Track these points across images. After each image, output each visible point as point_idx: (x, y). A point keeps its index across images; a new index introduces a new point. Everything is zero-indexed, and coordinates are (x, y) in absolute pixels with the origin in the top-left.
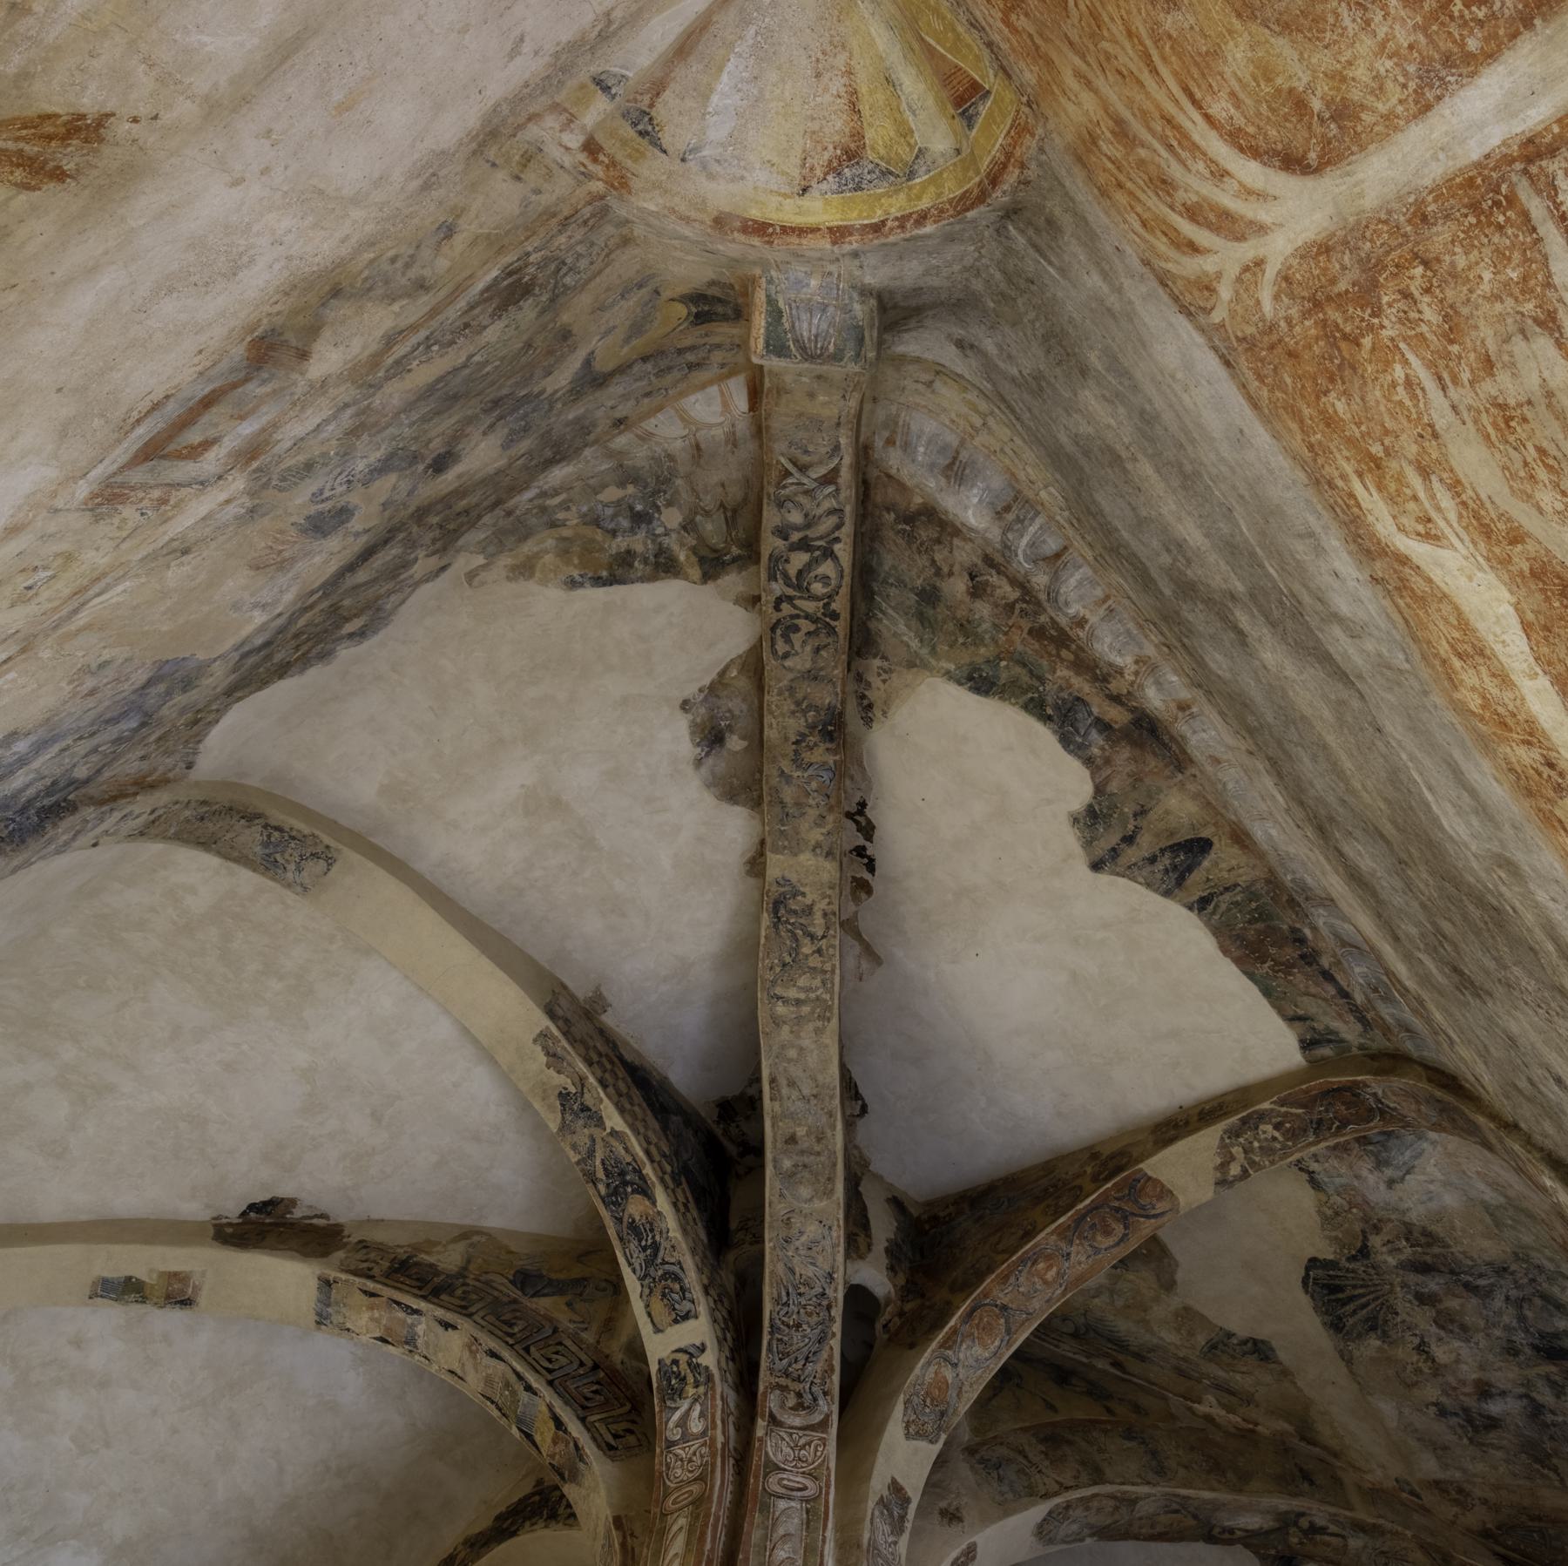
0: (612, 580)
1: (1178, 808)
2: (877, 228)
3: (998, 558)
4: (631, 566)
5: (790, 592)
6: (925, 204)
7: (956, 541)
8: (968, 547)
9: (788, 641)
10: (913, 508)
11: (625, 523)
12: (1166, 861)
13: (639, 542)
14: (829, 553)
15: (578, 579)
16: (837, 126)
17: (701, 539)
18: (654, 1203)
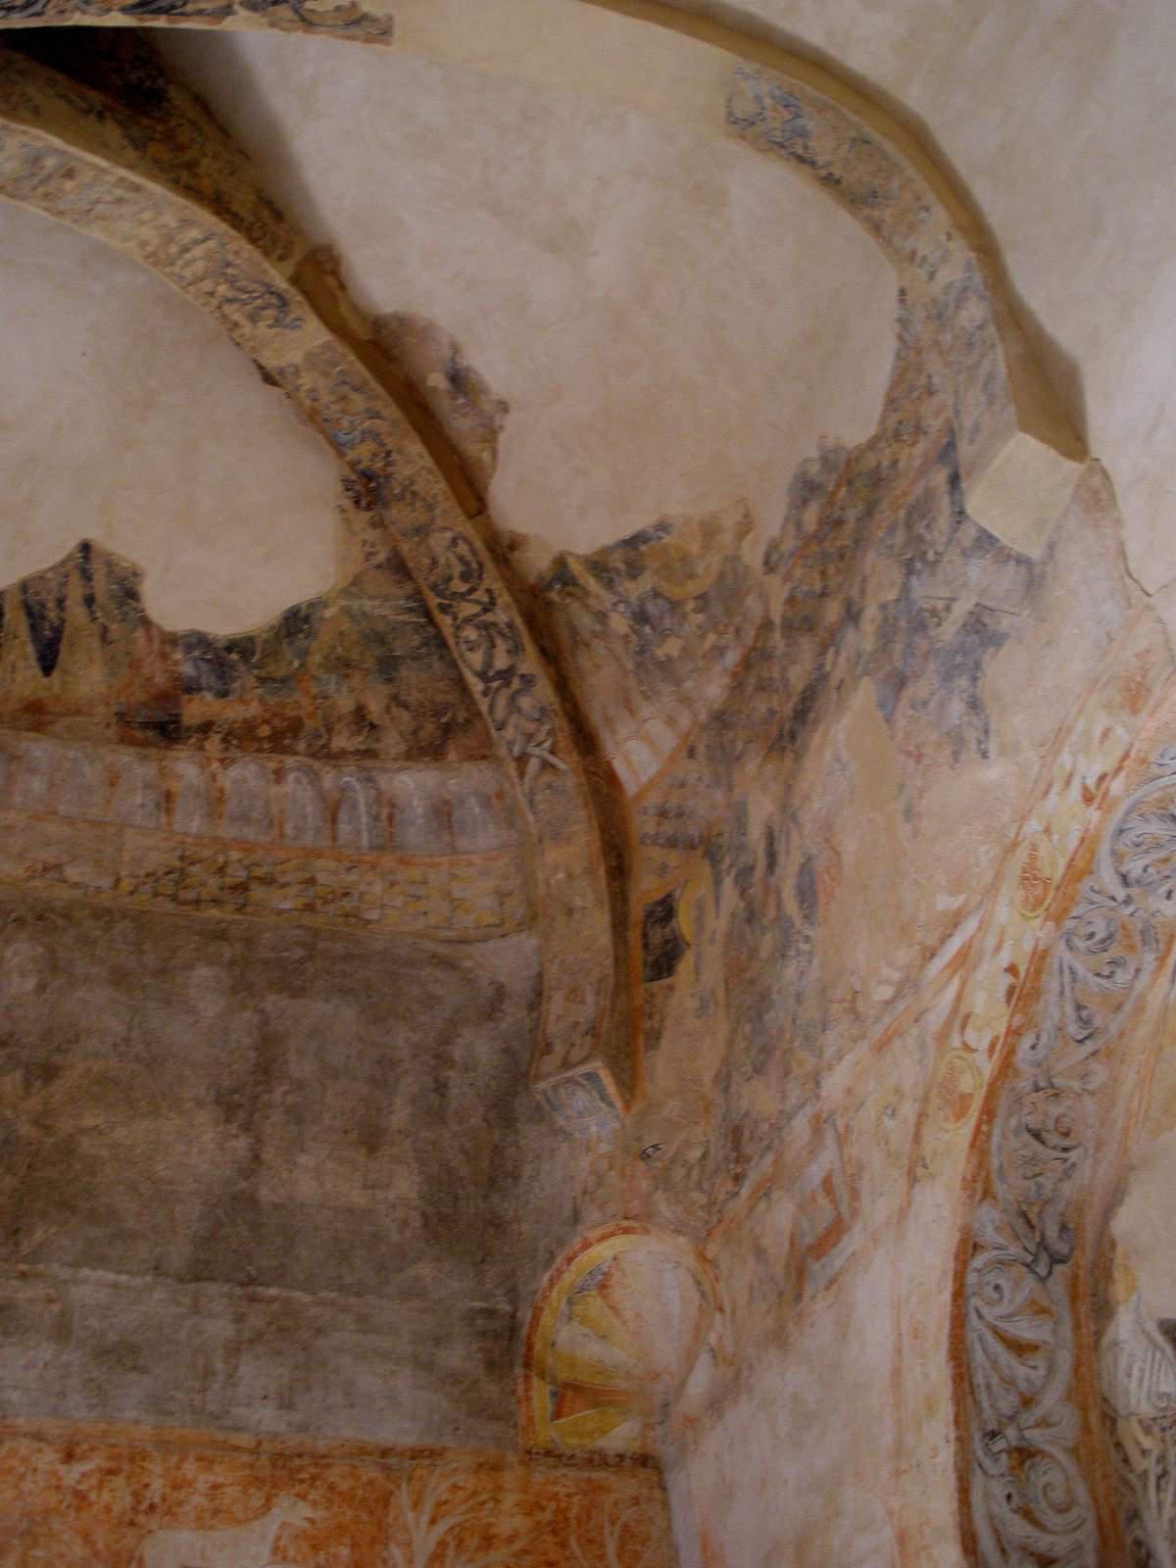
0: (633, 542)
1: (88, 676)
2: (570, 1260)
3: (368, 763)
4: (626, 563)
5: (488, 617)
6: (554, 1295)
7: (403, 747)
8: (393, 751)
9: (461, 559)
10: (451, 745)
11: (651, 608)
12: (52, 615)
13: (635, 590)
14: (482, 675)
15: (661, 534)
16: (617, 1294)
17: (586, 606)
18: (125, 10)
